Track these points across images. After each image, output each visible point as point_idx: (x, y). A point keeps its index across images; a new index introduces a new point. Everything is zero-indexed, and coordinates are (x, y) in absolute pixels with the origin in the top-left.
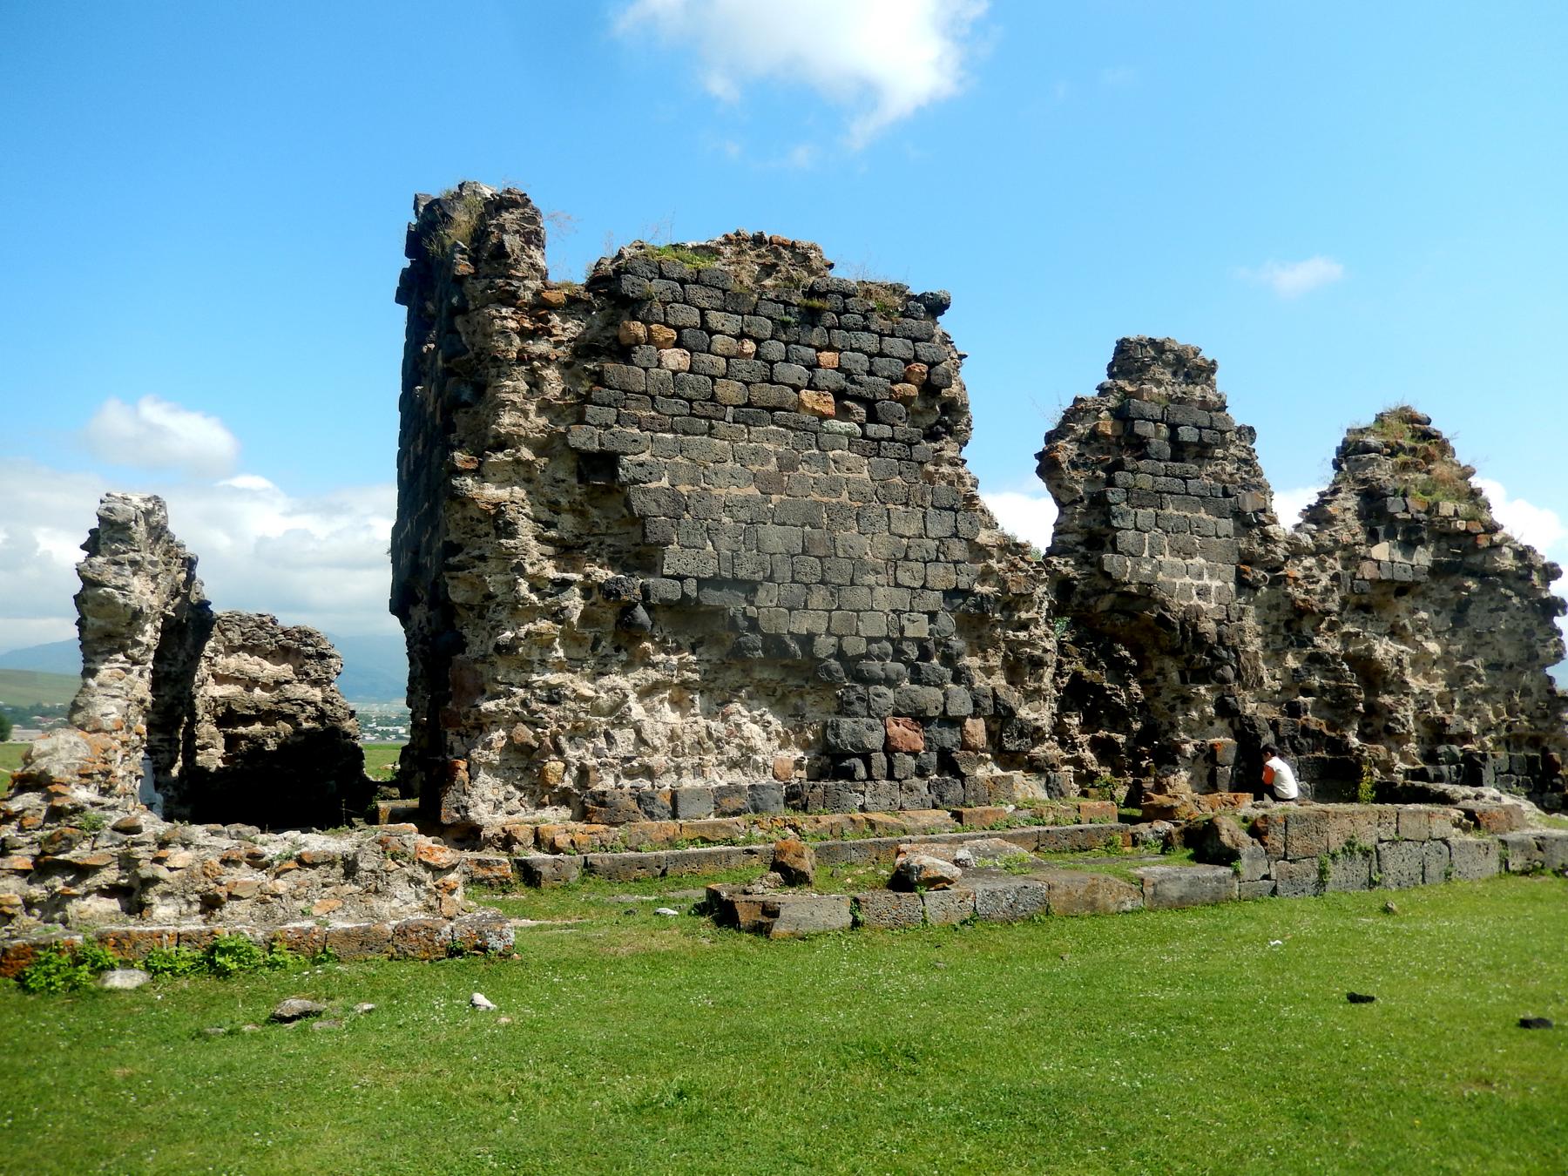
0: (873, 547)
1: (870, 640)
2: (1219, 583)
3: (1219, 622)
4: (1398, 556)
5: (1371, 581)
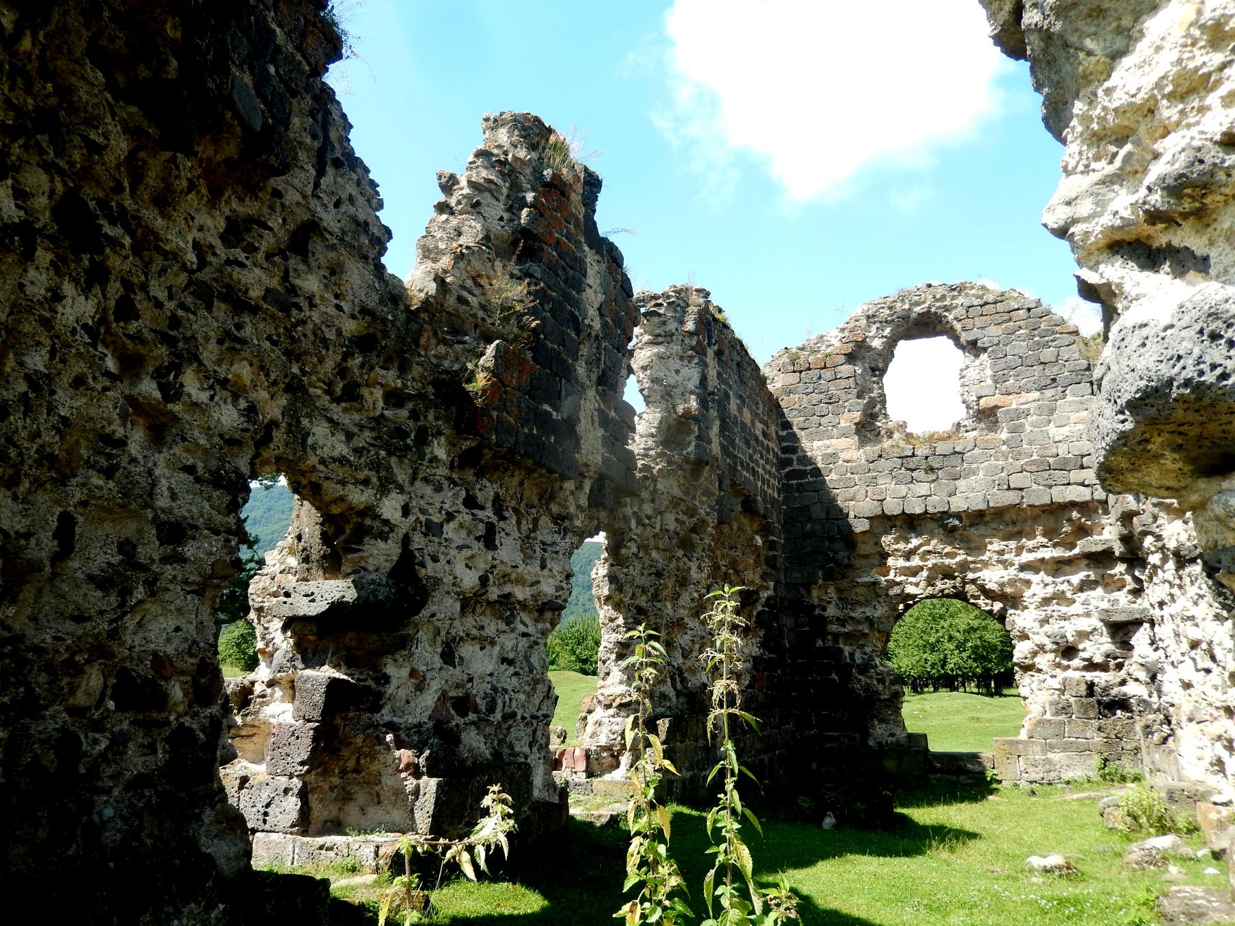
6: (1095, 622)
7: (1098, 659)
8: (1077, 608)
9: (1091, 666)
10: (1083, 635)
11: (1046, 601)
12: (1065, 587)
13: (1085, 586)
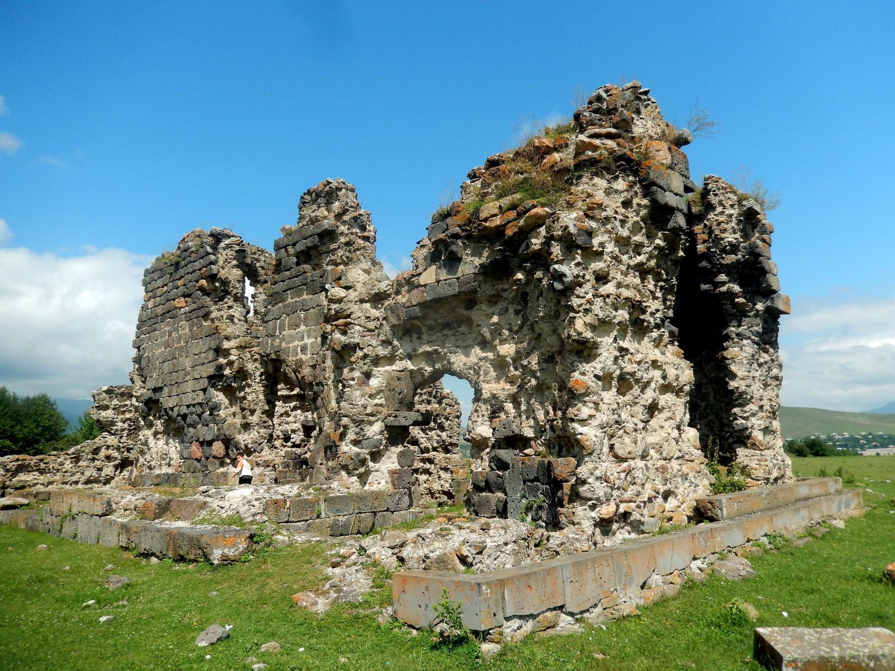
0: (187, 363)
1: (188, 406)
2: (313, 340)
3: (314, 367)
4: (444, 275)
5: (419, 304)
6: (297, 426)
7: (298, 442)
8: (291, 419)
9: (295, 445)
10: (294, 431)
11: (282, 415)
12: (288, 409)
13: (295, 408)
